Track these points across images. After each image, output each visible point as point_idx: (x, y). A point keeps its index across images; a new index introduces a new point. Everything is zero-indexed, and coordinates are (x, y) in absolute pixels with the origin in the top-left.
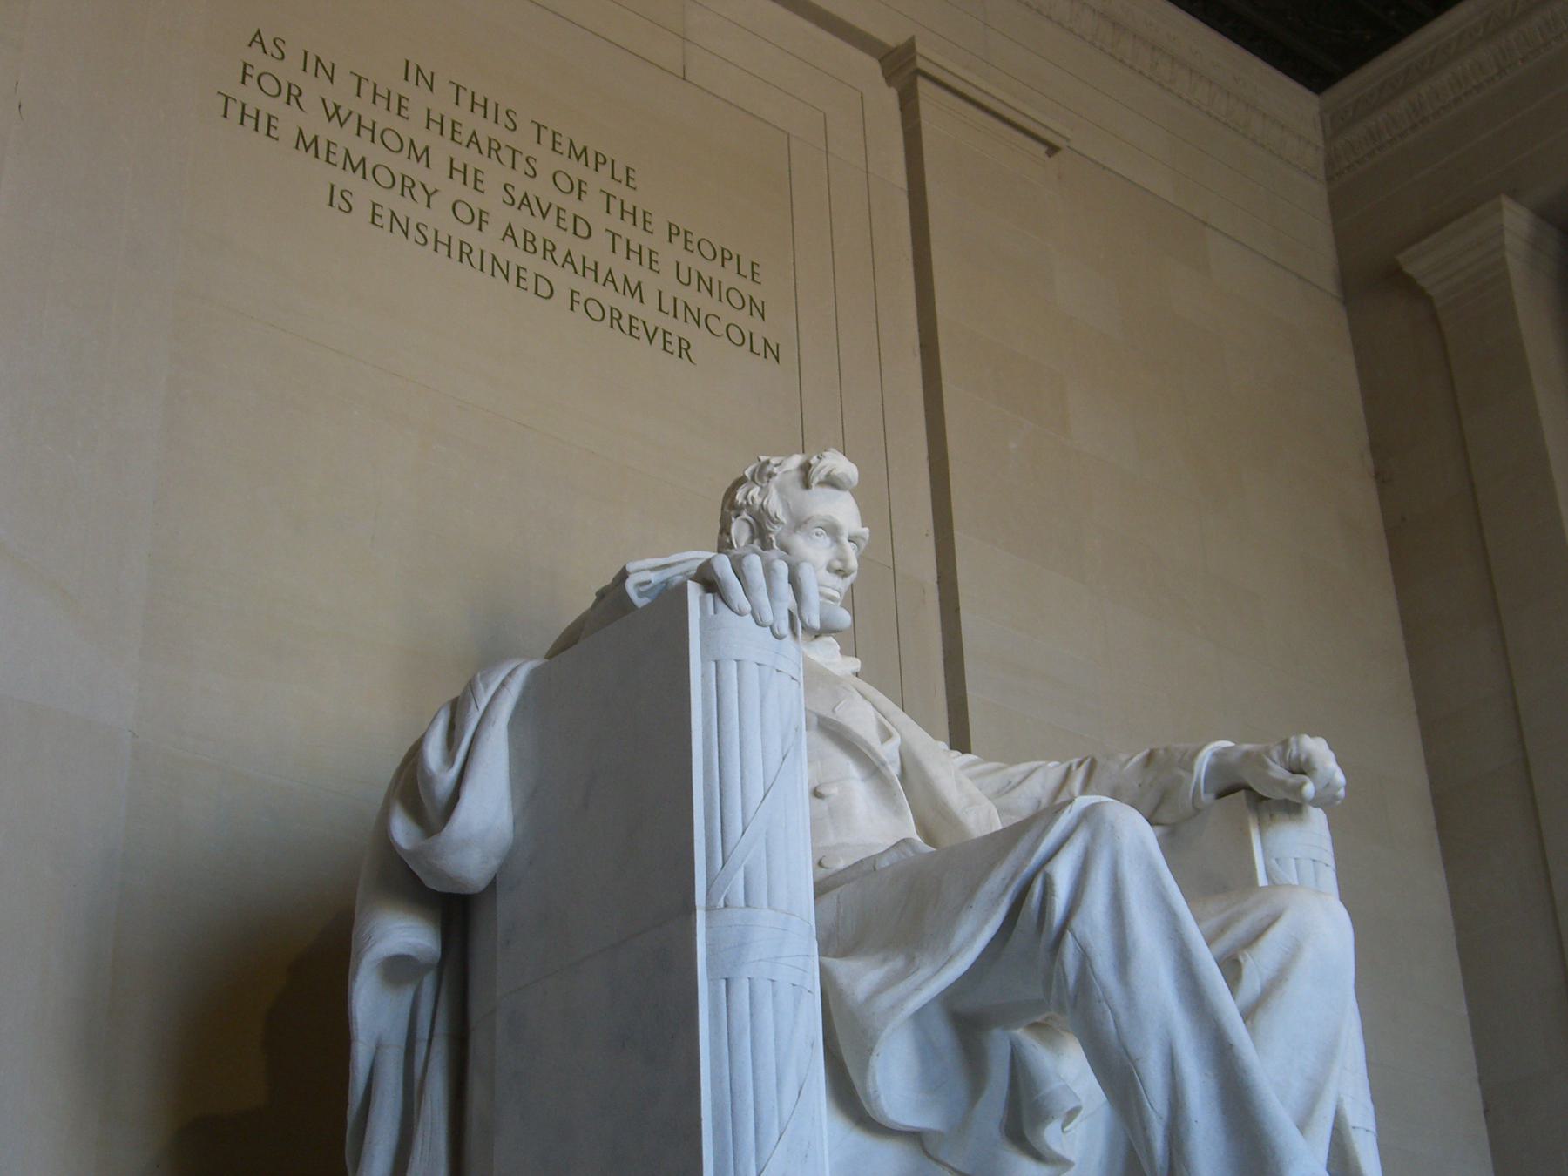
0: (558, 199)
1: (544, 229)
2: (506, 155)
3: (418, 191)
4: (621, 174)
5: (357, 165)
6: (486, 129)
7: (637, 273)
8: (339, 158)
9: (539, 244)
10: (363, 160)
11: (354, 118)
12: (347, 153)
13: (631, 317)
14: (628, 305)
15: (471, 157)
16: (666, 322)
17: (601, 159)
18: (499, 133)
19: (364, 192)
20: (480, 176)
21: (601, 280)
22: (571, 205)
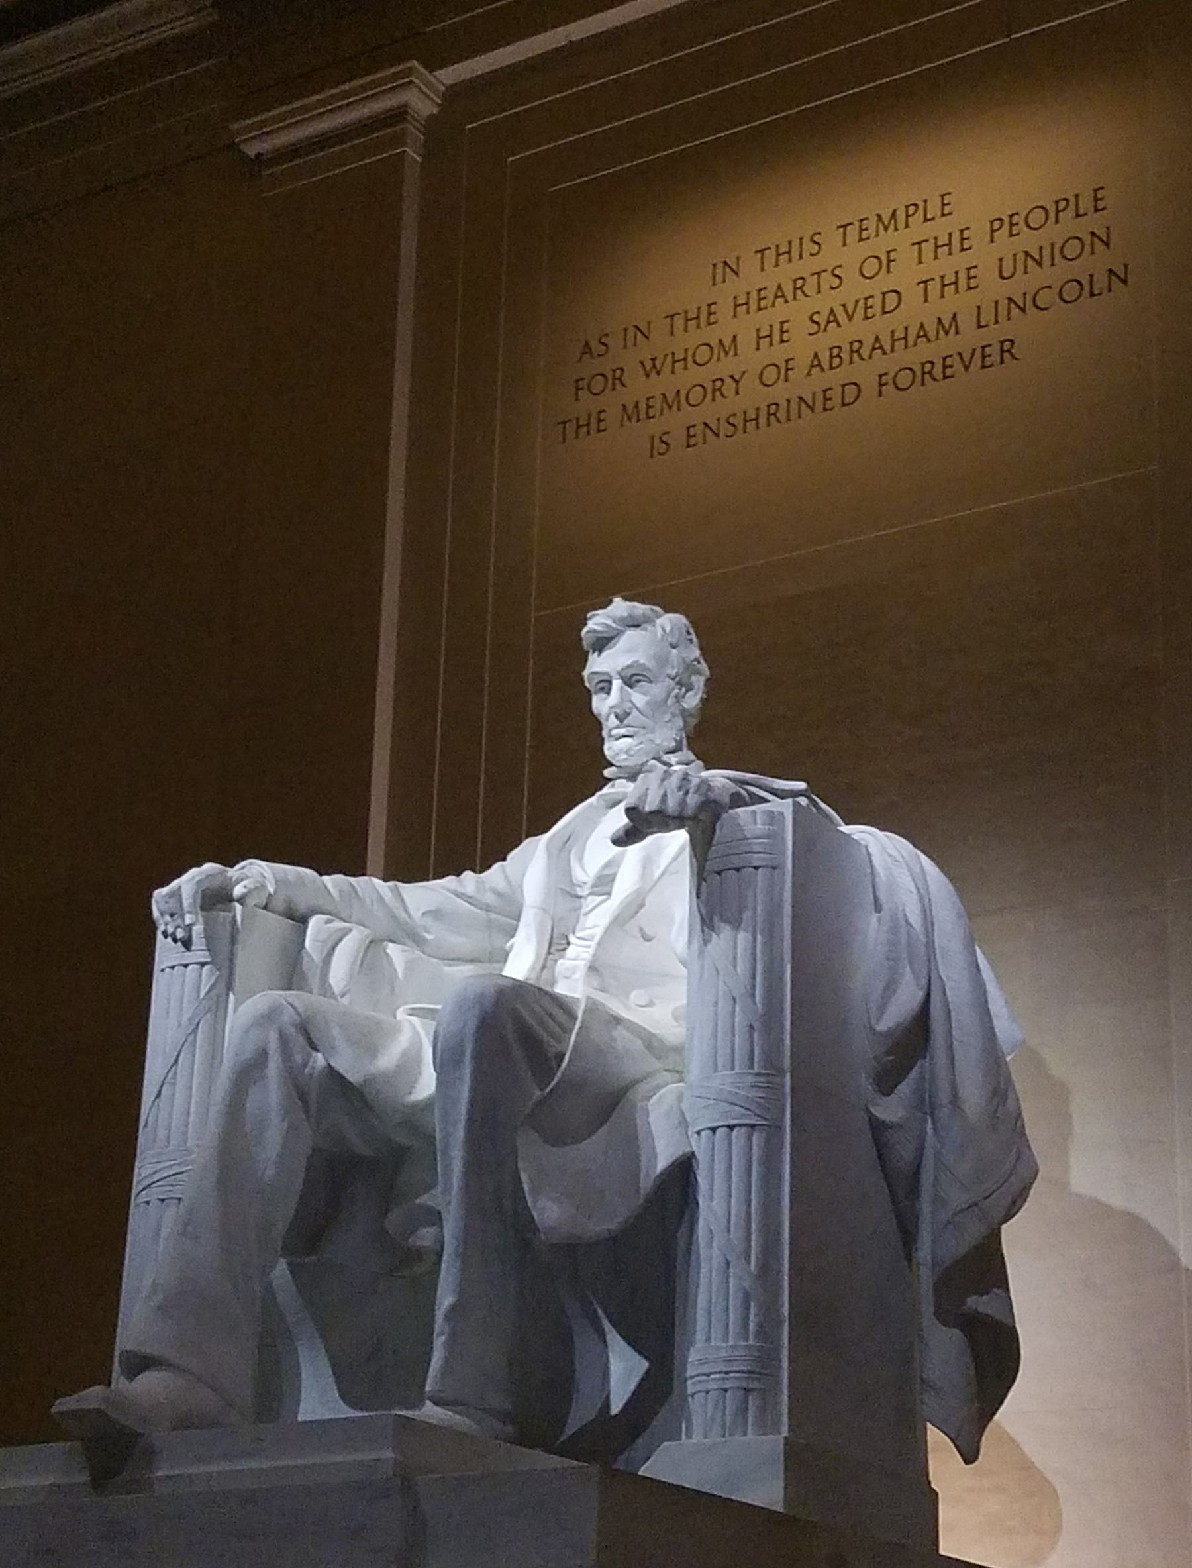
4: (934, 209)
5: (672, 402)
6: (786, 273)
19: (674, 422)
21: (911, 339)
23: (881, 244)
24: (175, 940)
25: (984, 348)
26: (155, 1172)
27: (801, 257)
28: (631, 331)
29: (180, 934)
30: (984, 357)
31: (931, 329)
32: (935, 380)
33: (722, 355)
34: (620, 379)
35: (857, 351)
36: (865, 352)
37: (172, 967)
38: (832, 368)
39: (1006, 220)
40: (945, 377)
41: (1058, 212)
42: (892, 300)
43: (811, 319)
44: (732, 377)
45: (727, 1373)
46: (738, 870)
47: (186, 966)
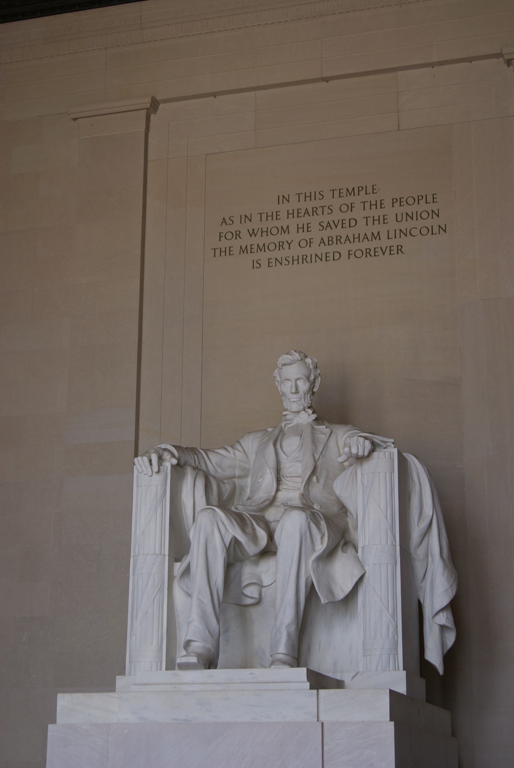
0: (342, 216)
2: (320, 211)
3: (286, 246)
4: (370, 190)
7: (376, 229)
9: (334, 240)
10: (264, 244)
11: (260, 230)
12: (258, 245)
13: (375, 248)
14: (373, 244)
15: (306, 220)
17: (360, 189)
18: (317, 203)
19: (264, 257)
20: (309, 225)
21: (361, 240)
22: (348, 215)
25: (390, 247)
27: (315, 199)
28: (243, 217)
30: (390, 250)
31: (369, 236)
32: (371, 255)
34: (239, 235)
35: (340, 240)
36: (343, 240)
40: (375, 255)
41: (419, 200)
42: (353, 223)
44: (287, 242)
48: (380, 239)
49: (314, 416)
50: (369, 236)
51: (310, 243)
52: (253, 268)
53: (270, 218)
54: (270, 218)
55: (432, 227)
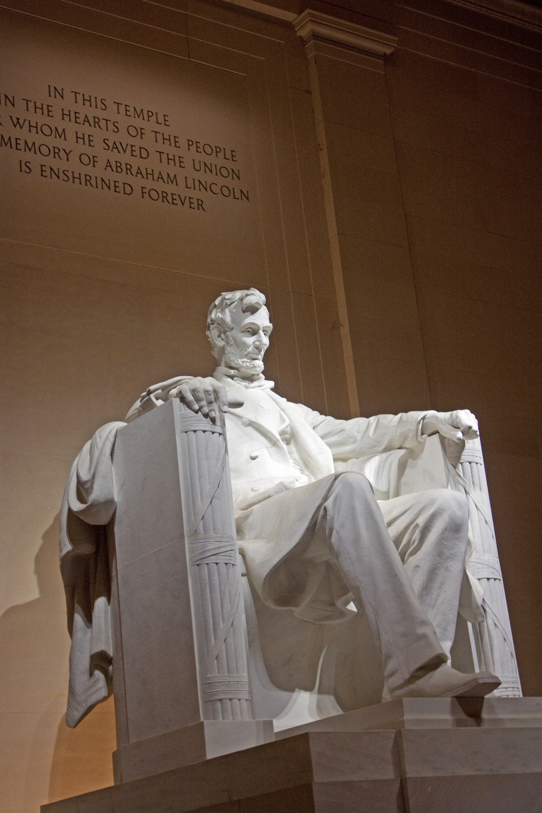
0: (131, 141)
1: (125, 158)
2: (103, 123)
3: (62, 154)
5: (30, 147)
7: (172, 170)
8: (22, 146)
9: (123, 167)
10: (34, 143)
11: (27, 122)
15: (86, 129)
16: (190, 193)
17: (150, 114)
19: (36, 160)
21: (156, 178)
22: (137, 142)
23: (138, 123)
24: (206, 416)
25: (190, 198)
26: (220, 548)
27: (96, 107)
29: (213, 414)
31: (165, 177)
33: (57, 136)
36: (134, 171)
37: (204, 431)
38: (117, 172)
39: (195, 143)
41: (217, 152)
42: (144, 154)
43: (104, 140)
44: (64, 150)
45: (513, 688)
46: (477, 463)
47: (213, 433)
48: (177, 185)
49: (272, 384)
50: (165, 177)
51: (94, 161)
52: (21, 171)
53: (39, 111)
54: (39, 111)
55: (233, 189)
